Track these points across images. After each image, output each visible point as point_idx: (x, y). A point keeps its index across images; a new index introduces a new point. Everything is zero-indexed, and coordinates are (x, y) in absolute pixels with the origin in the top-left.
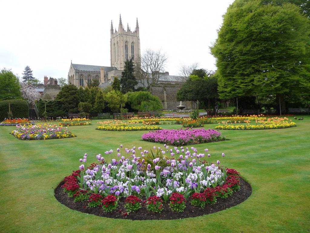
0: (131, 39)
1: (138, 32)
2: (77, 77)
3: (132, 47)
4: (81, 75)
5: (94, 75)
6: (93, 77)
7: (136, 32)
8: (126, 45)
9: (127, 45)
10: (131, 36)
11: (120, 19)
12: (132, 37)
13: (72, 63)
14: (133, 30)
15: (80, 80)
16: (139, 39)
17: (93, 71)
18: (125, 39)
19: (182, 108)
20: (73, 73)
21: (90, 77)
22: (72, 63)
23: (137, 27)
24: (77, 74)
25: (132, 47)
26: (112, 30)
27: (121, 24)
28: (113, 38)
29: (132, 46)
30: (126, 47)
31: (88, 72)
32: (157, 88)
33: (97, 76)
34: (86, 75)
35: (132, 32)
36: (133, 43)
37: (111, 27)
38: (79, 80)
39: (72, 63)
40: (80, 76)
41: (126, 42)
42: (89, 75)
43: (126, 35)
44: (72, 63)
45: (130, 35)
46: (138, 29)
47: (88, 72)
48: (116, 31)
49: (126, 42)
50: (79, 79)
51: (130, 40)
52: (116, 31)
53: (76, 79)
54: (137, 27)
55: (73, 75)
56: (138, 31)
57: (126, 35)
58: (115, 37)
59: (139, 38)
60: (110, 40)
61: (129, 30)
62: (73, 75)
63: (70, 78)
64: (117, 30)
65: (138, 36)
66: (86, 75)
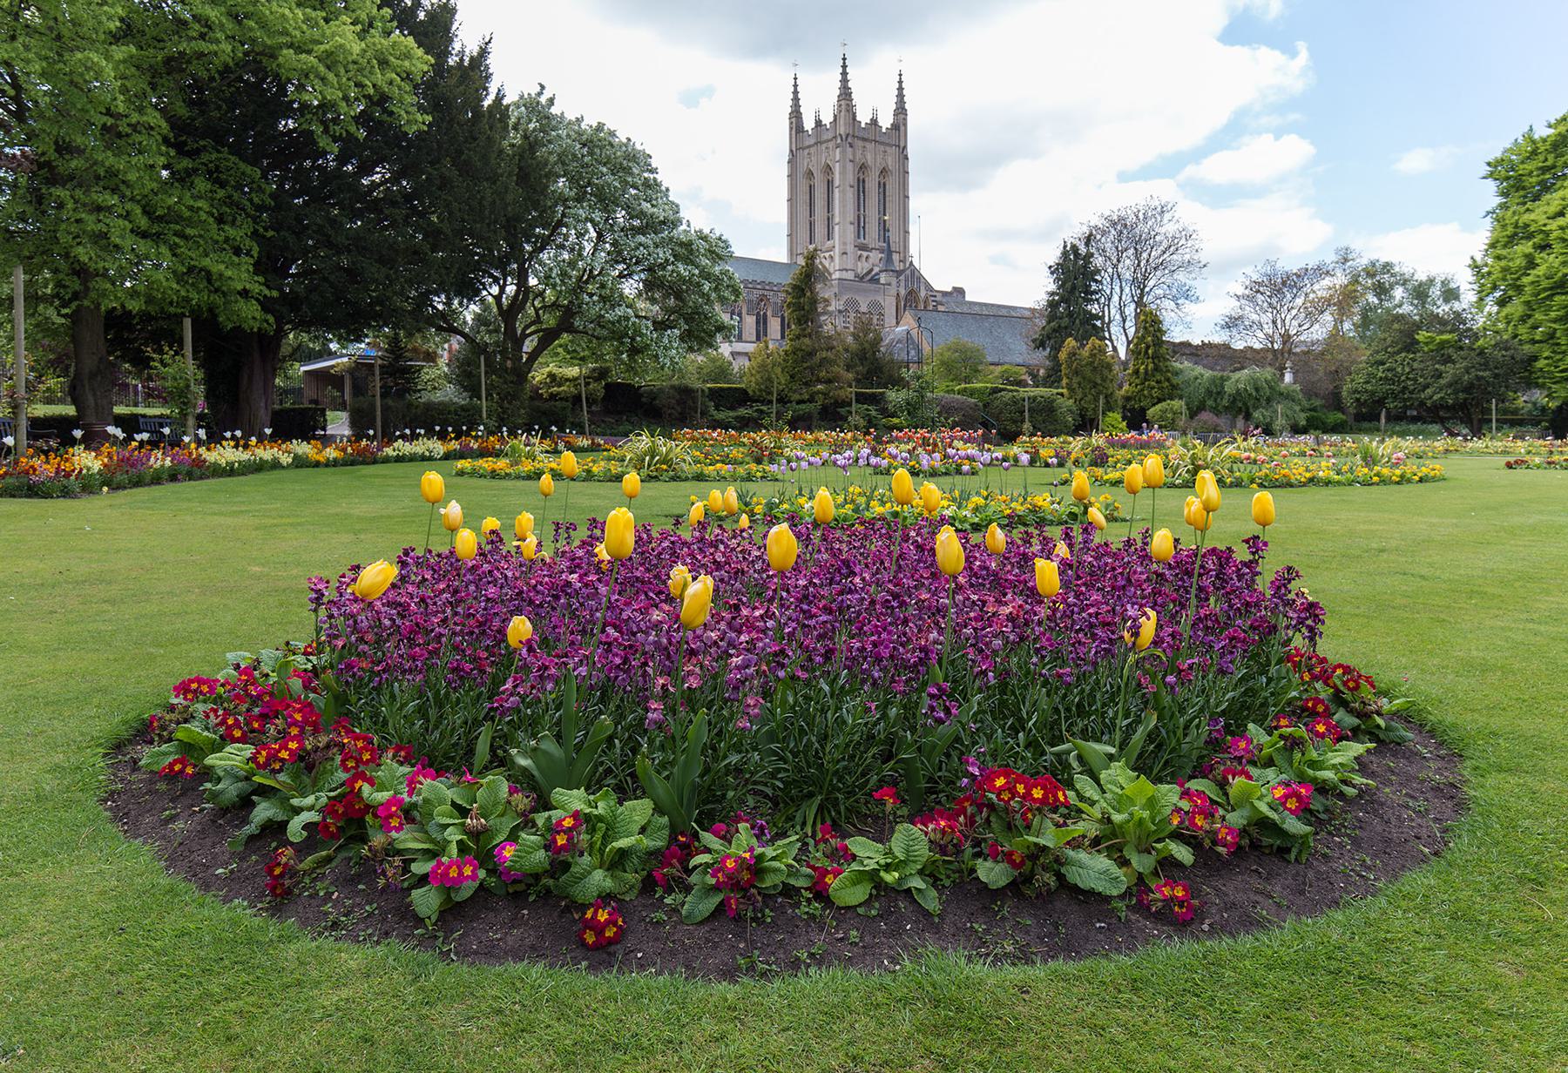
1: (902, 128)
3: (882, 187)
12: (882, 148)
16: (906, 158)
23: (901, 110)
25: (882, 187)
26: (796, 114)
27: (845, 94)
30: (860, 187)
36: (884, 172)
37: (790, 103)
41: (863, 168)
43: (864, 140)
46: (905, 119)
48: (819, 123)
52: (819, 123)
54: (901, 110)
57: (864, 140)
58: (809, 147)
60: (786, 156)
61: (874, 122)
64: (827, 119)
65: (902, 145)
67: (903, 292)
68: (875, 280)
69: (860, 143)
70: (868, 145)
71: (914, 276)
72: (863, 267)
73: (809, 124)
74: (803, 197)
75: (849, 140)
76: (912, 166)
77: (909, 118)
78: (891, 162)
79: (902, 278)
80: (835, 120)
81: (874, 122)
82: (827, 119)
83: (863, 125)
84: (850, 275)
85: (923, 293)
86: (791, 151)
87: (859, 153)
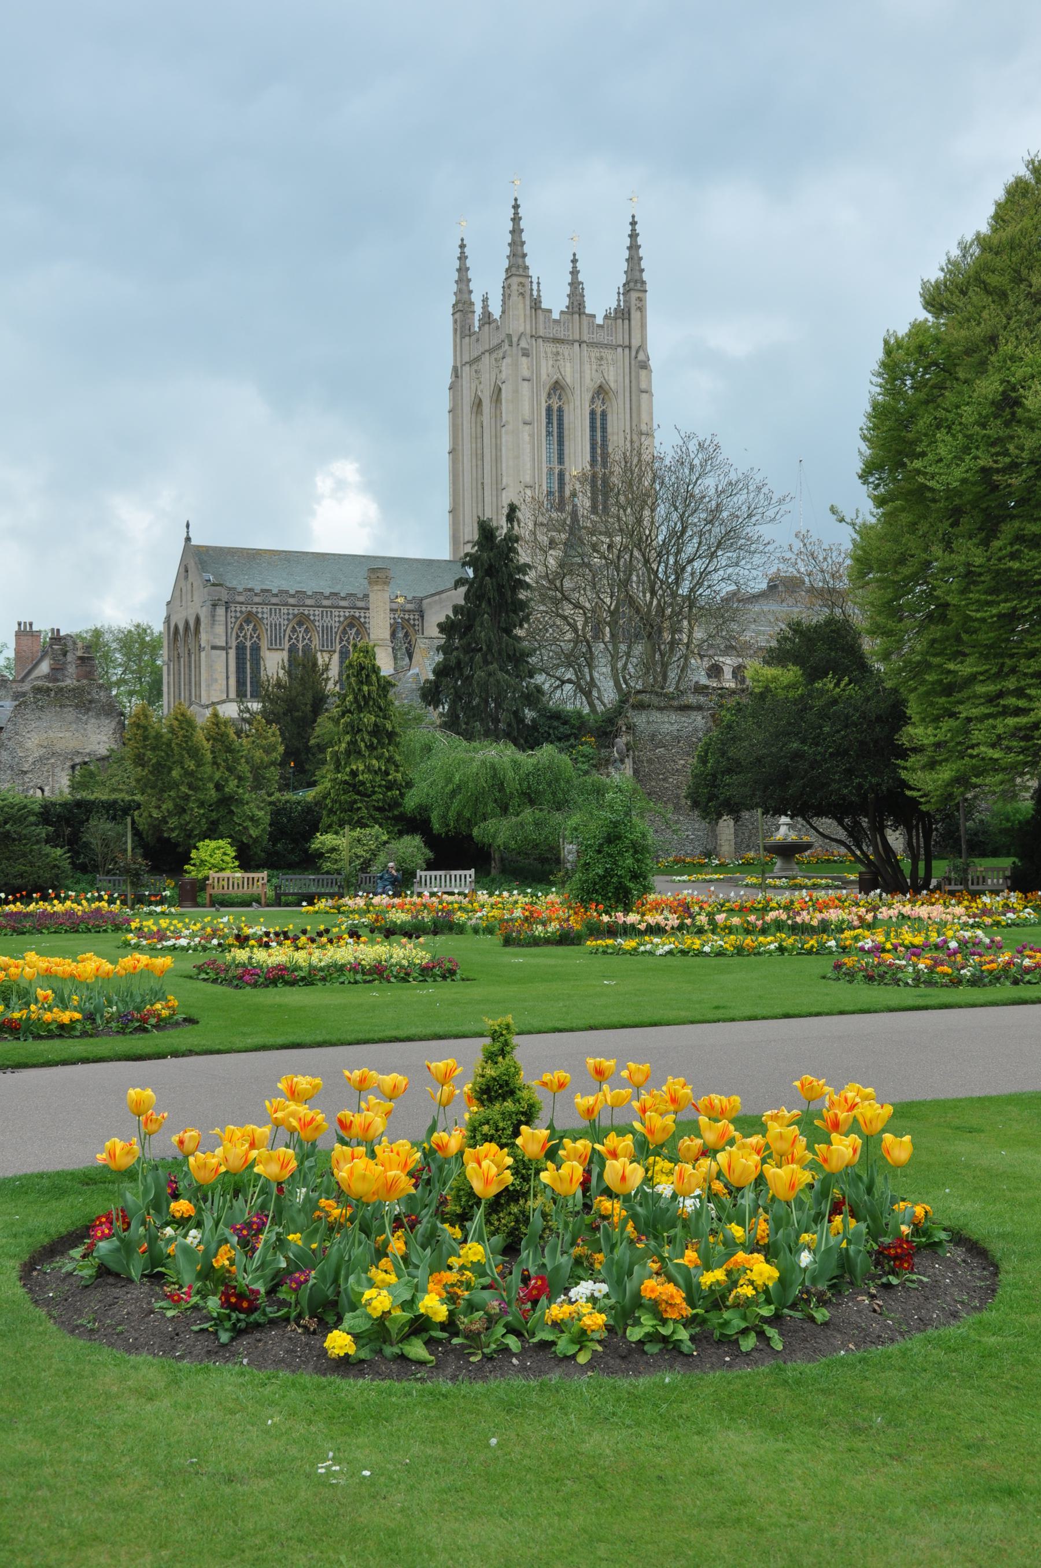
0: (587, 367)
1: (635, 315)
2: (220, 629)
3: (598, 423)
4: (249, 618)
5: (335, 620)
6: (327, 630)
8: (555, 407)
9: (560, 410)
10: (592, 345)
12: (595, 353)
13: (194, 542)
15: (240, 649)
16: (644, 366)
17: (327, 592)
18: (546, 372)
19: (787, 851)
20: (197, 606)
21: (307, 631)
22: (188, 539)
24: (221, 611)
26: (462, 307)
28: (470, 363)
29: (593, 413)
31: (291, 601)
32: (668, 723)
33: (351, 625)
34: (282, 618)
35: (599, 320)
36: (601, 392)
38: (232, 653)
39: (194, 542)
40: (241, 628)
41: (557, 388)
42: (302, 620)
44: (188, 539)
45: (581, 343)
46: (640, 299)
47: (291, 601)
49: (557, 388)
50: (234, 644)
52: (487, 316)
53: (214, 648)
55: (198, 620)
56: (641, 309)
59: (641, 357)
62: (198, 620)
63: (175, 639)
64: (496, 310)
65: (635, 343)
66: (275, 619)
69: (550, 348)
70: (564, 349)
74: (467, 448)
75: (523, 344)
77: (650, 297)
78: (614, 376)
80: (503, 312)
83: (556, 316)
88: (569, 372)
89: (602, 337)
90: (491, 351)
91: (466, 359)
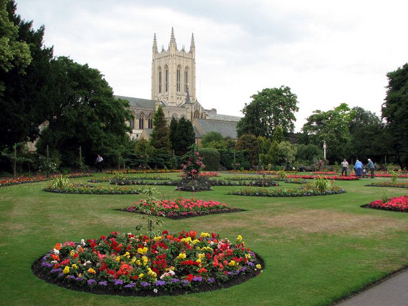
3: (186, 73)
7: (191, 52)
11: (173, 33)
14: (187, 50)
23: (193, 47)
25: (186, 73)
26: (155, 48)
27: (173, 40)
30: (178, 72)
36: (187, 67)
41: (179, 66)
48: (163, 50)
49: (179, 66)
51: (184, 64)
52: (163, 50)
54: (193, 47)
56: (194, 51)
60: (151, 61)
65: (193, 58)
67: (193, 111)
68: (184, 107)
69: (178, 58)
71: (197, 105)
72: (180, 102)
73: (160, 50)
74: (157, 77)
76: (197, 66)
77: (196, 49)
78: (189, 65)
79: (193, 106)
80: (169, 49)
81: (183, 50)
82: (166, 49)
84: (175, 105)
85: (201, 112)
86: (153, 60)
87: (177, 61)
88: (182, 64)
89: (187, 56)
90: (164, 57)
91: (157, 58)
